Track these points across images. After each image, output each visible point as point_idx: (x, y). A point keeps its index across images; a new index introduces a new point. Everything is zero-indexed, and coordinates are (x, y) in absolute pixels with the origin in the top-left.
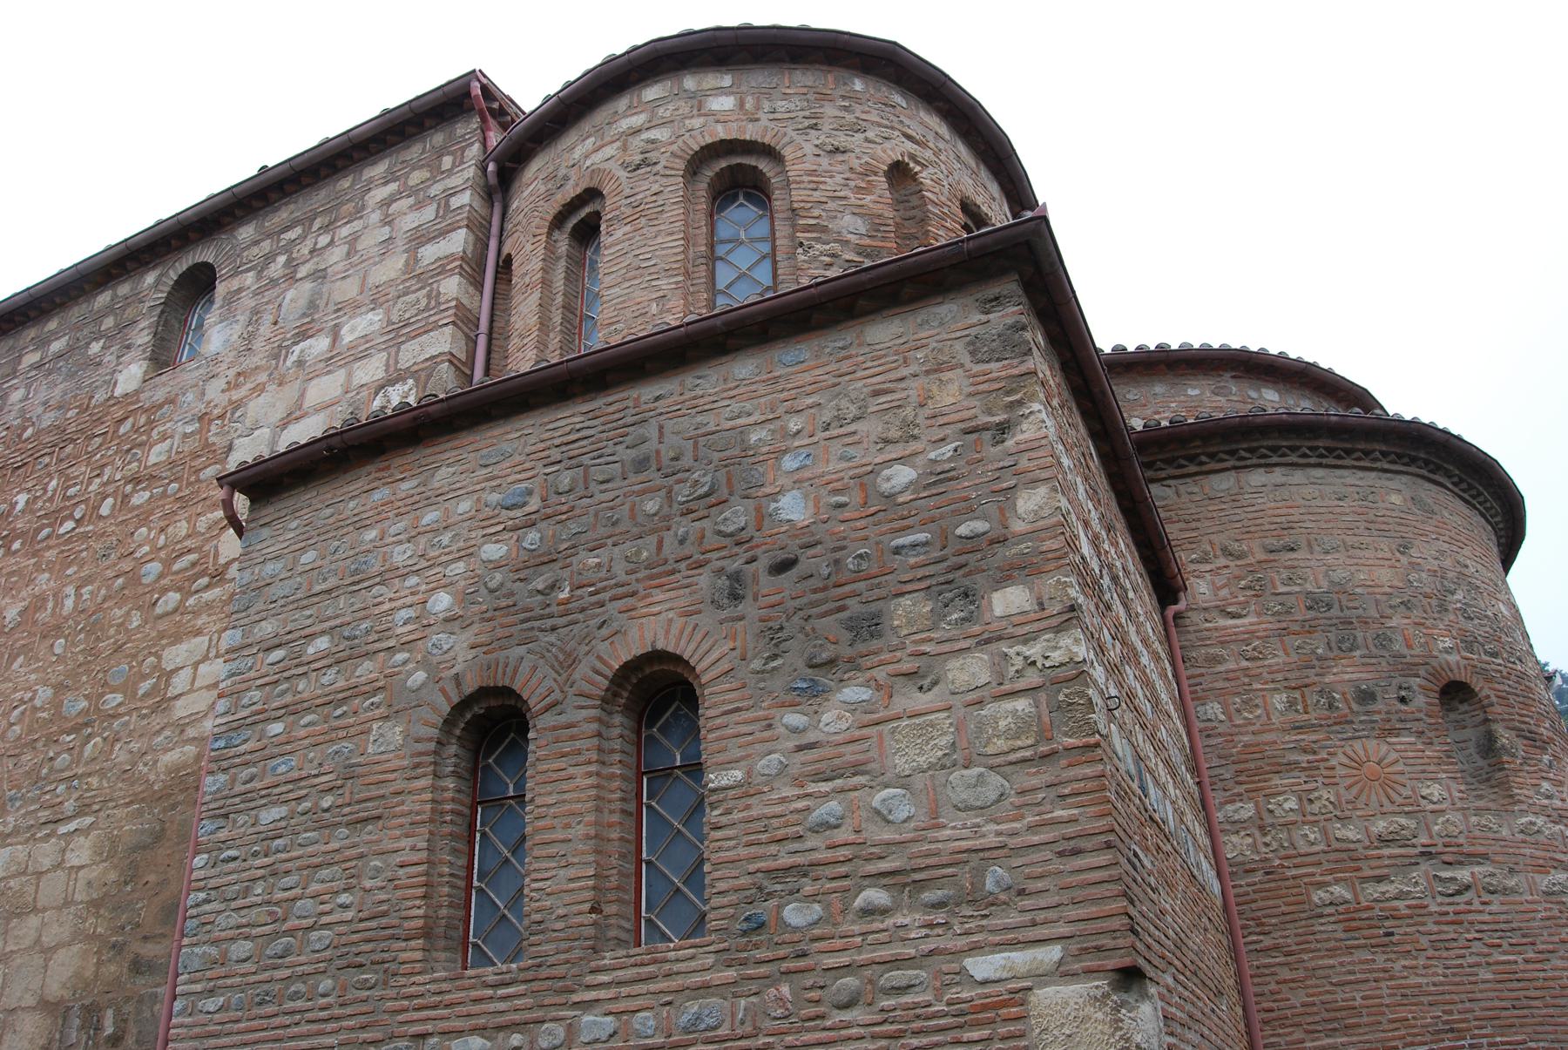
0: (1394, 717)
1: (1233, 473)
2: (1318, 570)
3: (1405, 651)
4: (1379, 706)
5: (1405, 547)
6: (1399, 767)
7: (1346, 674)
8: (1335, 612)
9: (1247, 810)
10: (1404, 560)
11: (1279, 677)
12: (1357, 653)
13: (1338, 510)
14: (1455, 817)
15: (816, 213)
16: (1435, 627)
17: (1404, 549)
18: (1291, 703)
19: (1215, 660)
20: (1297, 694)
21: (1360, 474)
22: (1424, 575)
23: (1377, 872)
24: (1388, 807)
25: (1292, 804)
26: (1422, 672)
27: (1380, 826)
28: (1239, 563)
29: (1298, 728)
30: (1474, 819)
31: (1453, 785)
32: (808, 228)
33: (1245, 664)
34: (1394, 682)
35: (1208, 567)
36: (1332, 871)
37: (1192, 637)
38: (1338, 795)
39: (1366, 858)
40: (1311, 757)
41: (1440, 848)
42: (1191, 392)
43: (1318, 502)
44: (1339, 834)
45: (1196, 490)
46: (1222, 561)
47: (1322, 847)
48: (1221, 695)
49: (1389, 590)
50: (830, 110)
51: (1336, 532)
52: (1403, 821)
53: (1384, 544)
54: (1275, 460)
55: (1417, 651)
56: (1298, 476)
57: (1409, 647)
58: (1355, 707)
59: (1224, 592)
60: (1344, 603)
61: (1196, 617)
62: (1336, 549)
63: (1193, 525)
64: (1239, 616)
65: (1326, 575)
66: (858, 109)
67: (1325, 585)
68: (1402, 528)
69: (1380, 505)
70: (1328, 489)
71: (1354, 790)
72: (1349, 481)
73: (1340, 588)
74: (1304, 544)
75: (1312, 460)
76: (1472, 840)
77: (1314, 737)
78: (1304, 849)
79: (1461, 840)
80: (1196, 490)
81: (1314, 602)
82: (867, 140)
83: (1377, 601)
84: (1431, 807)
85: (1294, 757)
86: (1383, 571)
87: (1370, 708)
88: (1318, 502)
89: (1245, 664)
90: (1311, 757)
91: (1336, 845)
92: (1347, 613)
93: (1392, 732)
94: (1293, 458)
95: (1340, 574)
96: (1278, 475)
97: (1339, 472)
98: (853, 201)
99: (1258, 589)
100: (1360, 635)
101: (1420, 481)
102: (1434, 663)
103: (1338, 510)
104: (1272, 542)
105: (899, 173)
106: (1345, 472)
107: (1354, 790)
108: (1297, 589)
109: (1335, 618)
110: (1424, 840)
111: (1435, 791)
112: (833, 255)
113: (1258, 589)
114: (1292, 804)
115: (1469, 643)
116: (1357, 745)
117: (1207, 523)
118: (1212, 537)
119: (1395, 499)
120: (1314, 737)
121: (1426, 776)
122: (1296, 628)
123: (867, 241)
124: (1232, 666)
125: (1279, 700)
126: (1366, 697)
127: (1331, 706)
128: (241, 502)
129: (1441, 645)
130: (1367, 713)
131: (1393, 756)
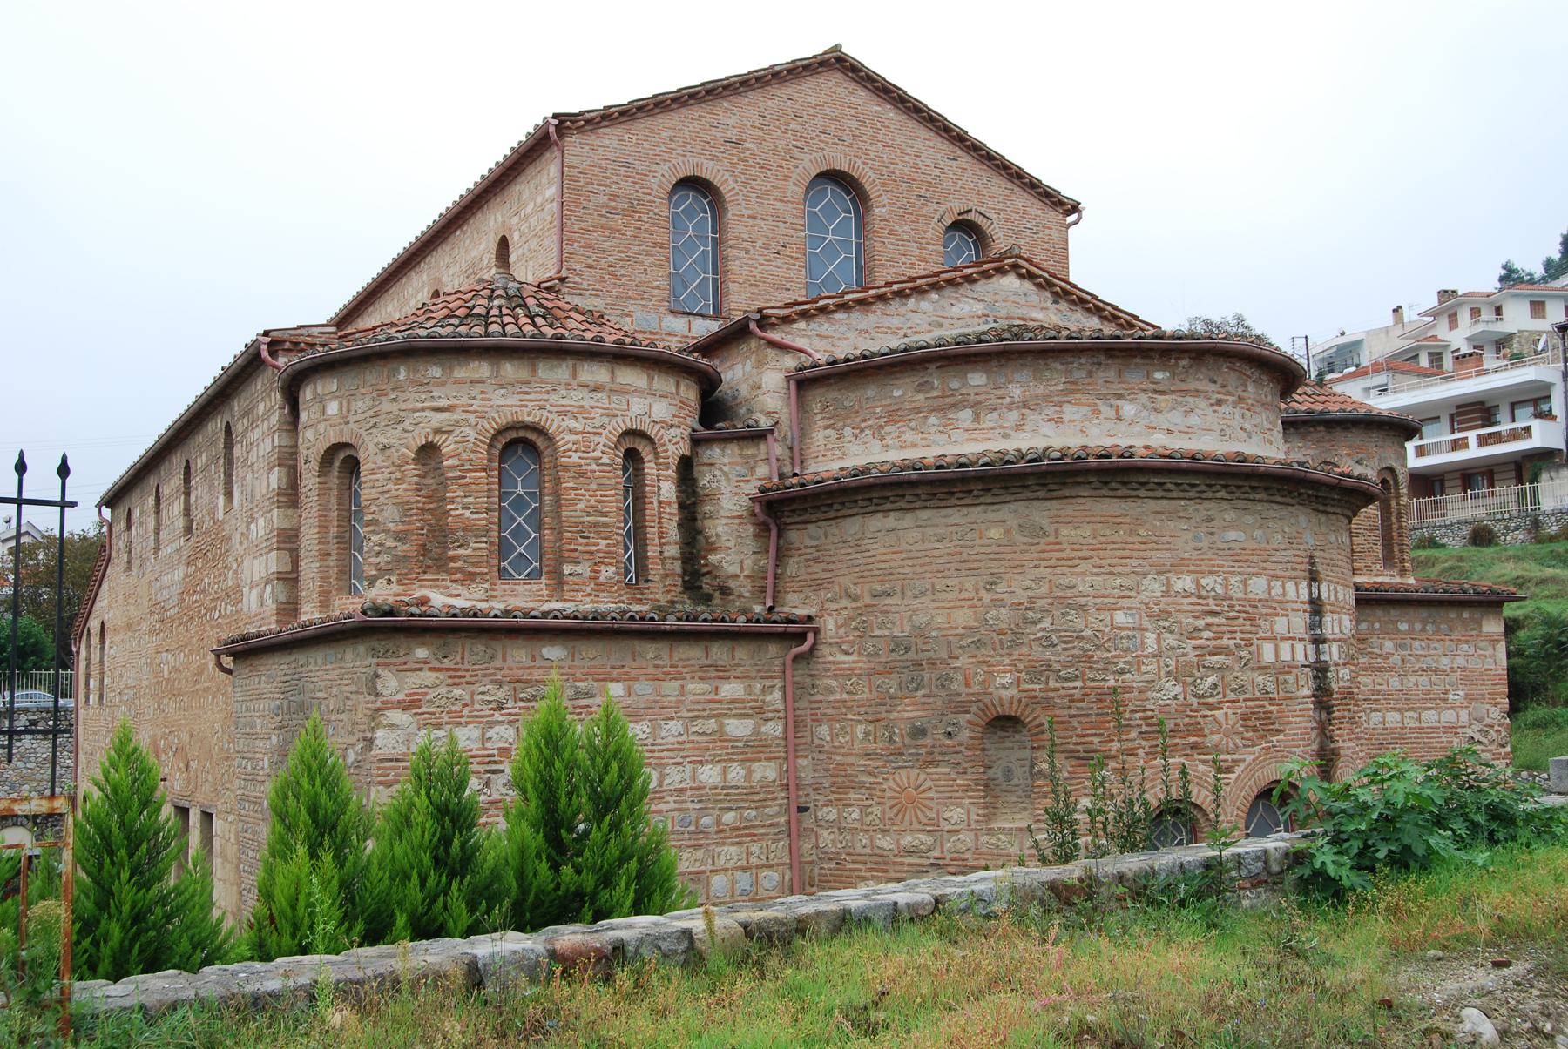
0: (936, 751)
1: (859, 518)
2: (904, 615)
3: (963, 690)
4: (928, 741)
5: (994, 583)
6: (931, 794)
7: (907, 712)
8: (911, 655)
9: (831, 813)
10: (987, 597)
11: (862, 710)
12: (920, 693)
13: (935, 553)
14: (967, 838)
15: (373, 508)
16: (999, 663)
17: (990, 586)
18: (867, 734)
19: (829, 690)
20: (871, 727)
21: (965, 510)
22: (1003, 611)
23: (899, 875)
24: (916, 826)
25: (856, 815)
26: (973, 709)
27: (907, 840)
28: (854, 605)
29: (868, 755)
30: (985, 838)
31: (974, 810)
32: (369, 523)
33: (845, 696)
34: (945, 719)
35: (834, 606)
36: (872, 870)
37: (820, 667)
38: (884, 812)
39: (895, 863)
40: (872, 780)
41: (947, 862)
42: (897, 393)
43: (917, 547)
44: (878, 843)
45: (836, 531)
46: (844, 603)
47: (867, 851)
48: (832, 719)
49: (960, 631)
50: (386, 406)
51: (928, 575)
52: (923, 837)
53: (969, 584)
54: (888, 506)
55: (975, 688)
56: (909, 519)
57: (968, 685)
58: (907, 741)
59: (842, 631)
60: (921, 646)
61: (824, 650)
62: (923, 593)
63: (832, 566)
64: (847, 653)
65: (910, 619)
66: (402, 396)
67: (907, 628)
68: (993, 564)
69: (978, 542)
70: (930, 531)
71: (895, 810)
72: (952, 520)
73: (920, 632)
74: (898, 589)
75: (917, 505)
76: (978, 854)
77: (876, 764)
78: (859, 850)
79: (967, 855)
80: (836, 531)
81: (897, 645)
82: (405, 431)
83: (949, 643)
84: (951, 827)
85: (863, 778)
86: (961, 612)
87: (920, 742)
88: (917, 547)
89: (845, 696)
90: (872, 780)
91: (877, 851)
92: (920, 655)
93: (931, 763)
94: (903, 504)
95: (921, 619)
96: (891, 521)
97: (944, 512)
98: (394, 493)
99: (863, 631)
100: (926, 676)
101: (1035, 503)
102: (987, 699)
103: (935, 553)
104: (877, 586)
105: (428, 451)
106: (949, 511)
107: (895, 810)
108: (886, 633)
109: (911, 661)
110: (937, 853)
111: (957, 814)
112: (381, 545)
113: (863, 631)
114: (856, 815)
115: (1040, 670)
116: (903, 773)
117: (839, 565)
118: (841, 579)
119: (995, 533)
120: (876, 764)
121: (950, 801)
122: (880, 668)
123: (401, 527)
124: (837, 697)
125: (860, 730)
126: (919, 732)
127: (890, 739)
128: (227, 661)
129: (999, 681)
130: (916, 747)
131: (929, 784)
